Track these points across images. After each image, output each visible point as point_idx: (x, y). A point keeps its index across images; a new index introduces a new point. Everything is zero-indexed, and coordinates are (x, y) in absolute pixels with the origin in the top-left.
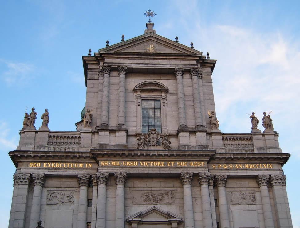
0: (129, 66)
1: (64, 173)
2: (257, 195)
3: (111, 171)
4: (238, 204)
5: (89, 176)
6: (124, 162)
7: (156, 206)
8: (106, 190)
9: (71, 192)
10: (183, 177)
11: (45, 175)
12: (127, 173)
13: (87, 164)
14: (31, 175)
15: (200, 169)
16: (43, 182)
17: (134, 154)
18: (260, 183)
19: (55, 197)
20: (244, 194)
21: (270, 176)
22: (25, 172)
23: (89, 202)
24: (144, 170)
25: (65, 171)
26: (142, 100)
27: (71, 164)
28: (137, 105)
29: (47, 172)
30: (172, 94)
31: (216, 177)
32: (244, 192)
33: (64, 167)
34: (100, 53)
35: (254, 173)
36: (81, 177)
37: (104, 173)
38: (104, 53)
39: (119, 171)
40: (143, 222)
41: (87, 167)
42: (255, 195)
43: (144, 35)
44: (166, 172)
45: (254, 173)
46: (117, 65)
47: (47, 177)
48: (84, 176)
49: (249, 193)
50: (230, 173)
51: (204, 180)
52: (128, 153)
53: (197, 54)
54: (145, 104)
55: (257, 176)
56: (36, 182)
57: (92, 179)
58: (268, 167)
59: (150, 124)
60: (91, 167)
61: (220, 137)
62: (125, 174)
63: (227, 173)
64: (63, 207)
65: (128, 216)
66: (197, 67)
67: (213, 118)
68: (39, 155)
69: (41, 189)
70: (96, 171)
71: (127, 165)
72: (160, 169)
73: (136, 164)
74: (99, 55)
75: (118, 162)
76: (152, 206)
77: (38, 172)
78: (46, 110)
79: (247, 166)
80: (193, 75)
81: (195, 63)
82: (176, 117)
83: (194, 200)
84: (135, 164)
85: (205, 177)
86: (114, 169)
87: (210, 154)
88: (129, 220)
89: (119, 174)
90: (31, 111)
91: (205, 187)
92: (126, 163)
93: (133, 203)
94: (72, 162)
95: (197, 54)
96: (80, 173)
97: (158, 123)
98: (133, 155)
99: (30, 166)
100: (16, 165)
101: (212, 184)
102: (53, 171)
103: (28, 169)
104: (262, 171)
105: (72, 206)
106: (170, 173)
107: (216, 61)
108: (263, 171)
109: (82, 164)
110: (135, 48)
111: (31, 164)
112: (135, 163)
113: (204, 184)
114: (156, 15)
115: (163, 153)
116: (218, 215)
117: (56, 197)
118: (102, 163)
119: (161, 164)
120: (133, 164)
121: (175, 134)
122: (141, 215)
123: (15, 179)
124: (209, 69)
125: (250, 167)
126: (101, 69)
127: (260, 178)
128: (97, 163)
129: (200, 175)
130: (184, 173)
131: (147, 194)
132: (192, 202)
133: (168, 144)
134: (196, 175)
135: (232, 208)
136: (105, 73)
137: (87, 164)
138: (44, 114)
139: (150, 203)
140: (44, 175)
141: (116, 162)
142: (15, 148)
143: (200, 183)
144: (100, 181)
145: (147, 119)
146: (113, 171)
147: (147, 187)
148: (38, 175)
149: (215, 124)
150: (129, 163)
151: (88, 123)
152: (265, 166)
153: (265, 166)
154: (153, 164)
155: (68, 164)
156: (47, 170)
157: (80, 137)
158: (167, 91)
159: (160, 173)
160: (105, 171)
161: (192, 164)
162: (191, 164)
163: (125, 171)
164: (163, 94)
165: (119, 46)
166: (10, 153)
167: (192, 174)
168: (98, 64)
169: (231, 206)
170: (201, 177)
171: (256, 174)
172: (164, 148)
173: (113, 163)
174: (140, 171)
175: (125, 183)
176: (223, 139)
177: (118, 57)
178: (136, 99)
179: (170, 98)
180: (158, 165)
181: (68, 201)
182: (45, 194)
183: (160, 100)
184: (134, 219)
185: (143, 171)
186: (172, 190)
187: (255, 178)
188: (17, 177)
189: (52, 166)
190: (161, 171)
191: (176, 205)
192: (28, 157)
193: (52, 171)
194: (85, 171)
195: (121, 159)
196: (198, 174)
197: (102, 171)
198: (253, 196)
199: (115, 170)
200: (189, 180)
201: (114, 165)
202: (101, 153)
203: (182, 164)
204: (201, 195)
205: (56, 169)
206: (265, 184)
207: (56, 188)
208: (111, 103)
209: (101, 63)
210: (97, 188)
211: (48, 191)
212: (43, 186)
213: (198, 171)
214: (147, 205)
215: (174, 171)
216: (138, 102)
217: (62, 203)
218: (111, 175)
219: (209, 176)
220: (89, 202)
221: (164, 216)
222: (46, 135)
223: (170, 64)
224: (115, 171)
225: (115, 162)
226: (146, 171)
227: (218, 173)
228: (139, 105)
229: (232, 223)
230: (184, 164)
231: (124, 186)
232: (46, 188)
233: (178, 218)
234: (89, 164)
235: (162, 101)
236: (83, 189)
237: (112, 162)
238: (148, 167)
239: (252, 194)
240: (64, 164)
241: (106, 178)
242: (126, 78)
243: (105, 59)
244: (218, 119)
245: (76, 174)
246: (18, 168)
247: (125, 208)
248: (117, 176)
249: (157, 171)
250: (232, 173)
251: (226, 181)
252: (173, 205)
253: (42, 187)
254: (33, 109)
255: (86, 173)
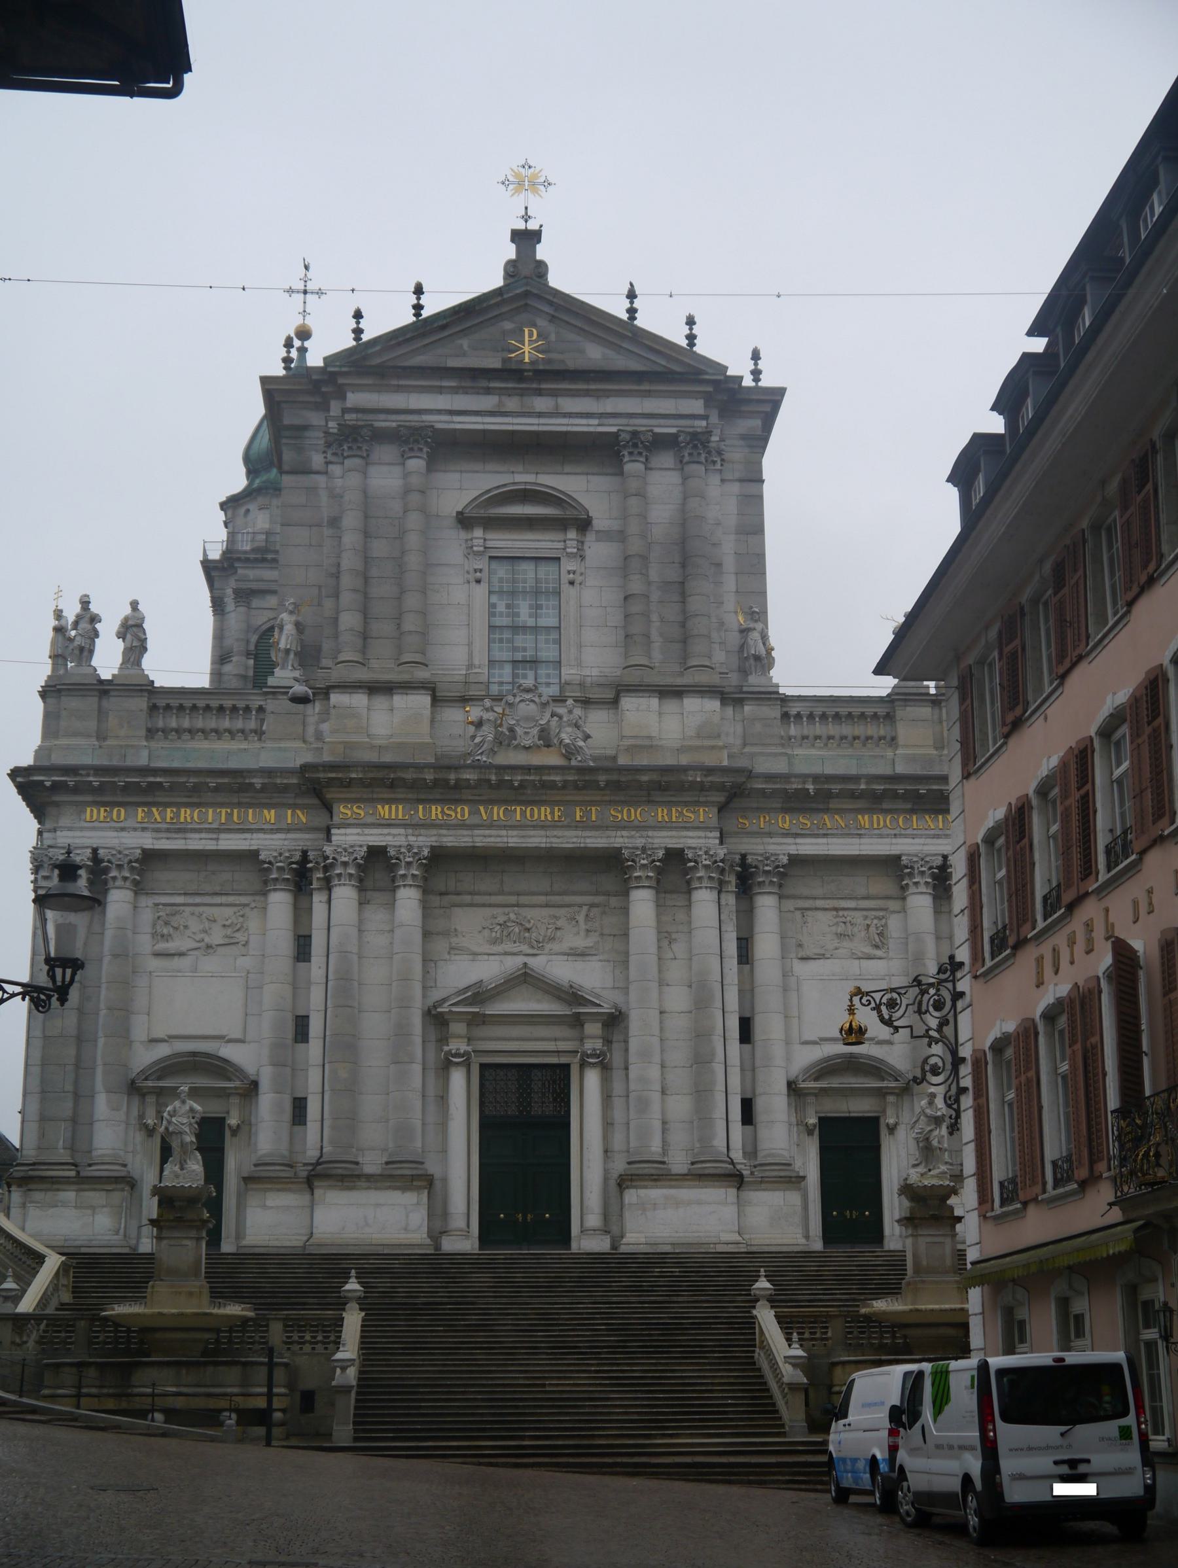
0: (442, 422)
1: (210, 845)
2: (894, 924)
3: (376, 837)
4: (822, 957)
5: (297, 856)
6: (421, 807)
7: (531, 961)
8: (360, 904)
9: (235, 909)
10: (630, 863)
11: (144, 851)
12: (432, 847)
13: (289, 812)
14: (95, 851)
15: (690, 834)
16: (137, 877)
17: (457, 780)
18: (905, 882)
19: (182, 927)
20: (848, 918)
21: (945, 857)
22: (69, 841)
23: (302, 949)
24: (490, 836)
25: (214, 836)
26: (491, 558)
27: (235, 811)
28: (471, 577)
29: (150, 841)
30: (606, 536)
31: (750, 859)
32: (846, 913)
33: (210, 820)
34: (330, 369)
35: (888, 847)
36: (272, 860)
37: (352, 846)
38: (344, 369)
39: (403, 839)
40: (485, 1015)
41: (289, 822)
42: (885, 925)
43: (498, 292)
44: (567, 843)
45: (888, 847)
46: (394, 417)
47: (150, 857)
48: (281, 854)
49: (866, 917)
50: (800, 844)
51: (701, 873)
52: (437, 777)
53: (707, 373)
54: (502, 571)
55: (898, 858)
56: (114, 878)
57: (310, 865)
58: (941, 826)
59: (519, 656)
60: (304, 820)
61: (775, 712)
62: (426, 852)
63: (789, 844)
64: (210, 964)
65: (436, 995)
66: (704, 423)
67: (755, 635)
68: (121, 780)
69: (132, 900)
70: (322, 836)
71: (433, 817)
72: (548, 833)
73: (463, 815)
74: (326, 377)
75: (400, 807)
76: (520, 960)
77: (117, 841)
78: (134, 605)
79: (864, 820)
80: (687, 459)
81: (696, 406)
82: (616, 627)
83: (665, 943)
84: (463, 812)
85: (708, 862)
86: (386, 831)
87: (728, 780)
88: (439, 1010)
89: (403, 850)
90: (77, 608)
91: (705, 902)
92: (430, 808)
93: (452, 949)
94: (239, 805)
95: (707, 373)
96: (267, 843)
97: (547, 652)
98: (452, 782)
99: (88, 818)
100: (39, 810)
101: (732, 887)
102: (169, 835)
103: (82, 829)
104: (917, 841)
105: (241, 961)
106: (582, 845)
107: (781, 392)
108: (922, 841)
109: (273, 812)
110: (465, 343)
111: (92, 811)
112: (459, 810)
113: (701, 888)
114: (550, 188)
115: (558, 778)
116: (747, 992)
117: (186, 927)
118: (343, 811)
119: (552, 813)
120: (453, 814)
121: (610, 695)
122: (479, 995)
123: (36, 870)
124: (757, 423)
125: (875, 826)
126: (335, 431)
127: (907, 867)
128: (328, 808)
129: (690, 856)
130: (633, 848)
131: (501, 919)
132: (659, 947)
133: (581, 743)
134: (675, 857)
135: (800, 968)
136: (350, 453)
137: (289, 812)
138: (126, 619)
139: (516, 950)
140: (139, 851)
141: (394, 807)
142: (27, 760)
143: (688, 882)
144: (339, 875)
145: (507, 635)
146: (382, 838)
147: (501, 893)
148: (120, 852)
149: (757, 658)
150: (439, 809)
151: (292, 656)
152: (930, 823)
153: (930, 823)
154: (523, 813)
155: (224, 811)
156: (148, 834)
157: (261, 709)
158: (584, 524)
159: (548, 845)
160: (356, 838)
161: (661, 813)
162: (660, 815)
163: (424, 841)
164: (572, 534)
165: (401, 339)
166: (14, 773)
167: (661, 854)
168: (324, 407)
169: (795, 961)
170: (692, 864)
171: (895, 850)
172: (564, 755)
173: (384, 811)
174: (477, 839)
175: (425, 879)
176: (785, 716)
177: (398, 386)
178: (466, 556)
179: (598, 551)
180: (543, 818)
181: (227, 941)
182: (147, 916)
183: (559, 559)
184: (455, 1009)
185: (489, 840)
186: (592, 906)
187: (892, 865)
188: (45, 859)
189: (168, 820)
190: (554, 840)
191: (601, 957)
192: (77, 790)
193: (168, 839)
194: (282, 836)
195: (410, 796)
196: (682, 850)
197: (343, 838)
198: (877, 928)
199: (389, 834)
200: (651, 874)
201: (387, 817)
202: (340, 775)
203: (629, 815)
204: (690, 923)
205: (179, 831)
206: (923, 889)
207: (185, 894)
208: (374, 572)
209: (335, 408)
210: (324, 898)
211: (157, 905)
212: (139, 888)
213: (682, 840)
214: (502, 957)
215: (599, 840)
216: (476, 571)
217: (209, 947)
218: (376, 854)
219: (722, 861)
220: (302, 949)
221: (559, 998)
222: (141, 703)
223: (601, 415)
224: (390, 838)
225: (390, 809)
226: (499, 840)
227: (756, 848)
228: (478, 581)
229: (795, 1021)
230: (635, 814)
231: (421, 891)
232: (147, 894)
233: (605, 1005)
234: (299, 812)
235: (568, 565)
236: (280, 902)
237: (379, 807)
238: (505, 826)
239: (875, 921)
240: (211, 811)
241: (359, 866)
242: (430, 468)
243: (350, 395)
244: (773, 641)
245: (252, 848)
246: (49, 825)
247: (424, 966)
248: (397, 859)
249: (536, 840)
250: (808, 847)
251: (783, 875)
252: (588, 958)
253: (136, 893)
254: (85, 603)
255: (286, 843)
